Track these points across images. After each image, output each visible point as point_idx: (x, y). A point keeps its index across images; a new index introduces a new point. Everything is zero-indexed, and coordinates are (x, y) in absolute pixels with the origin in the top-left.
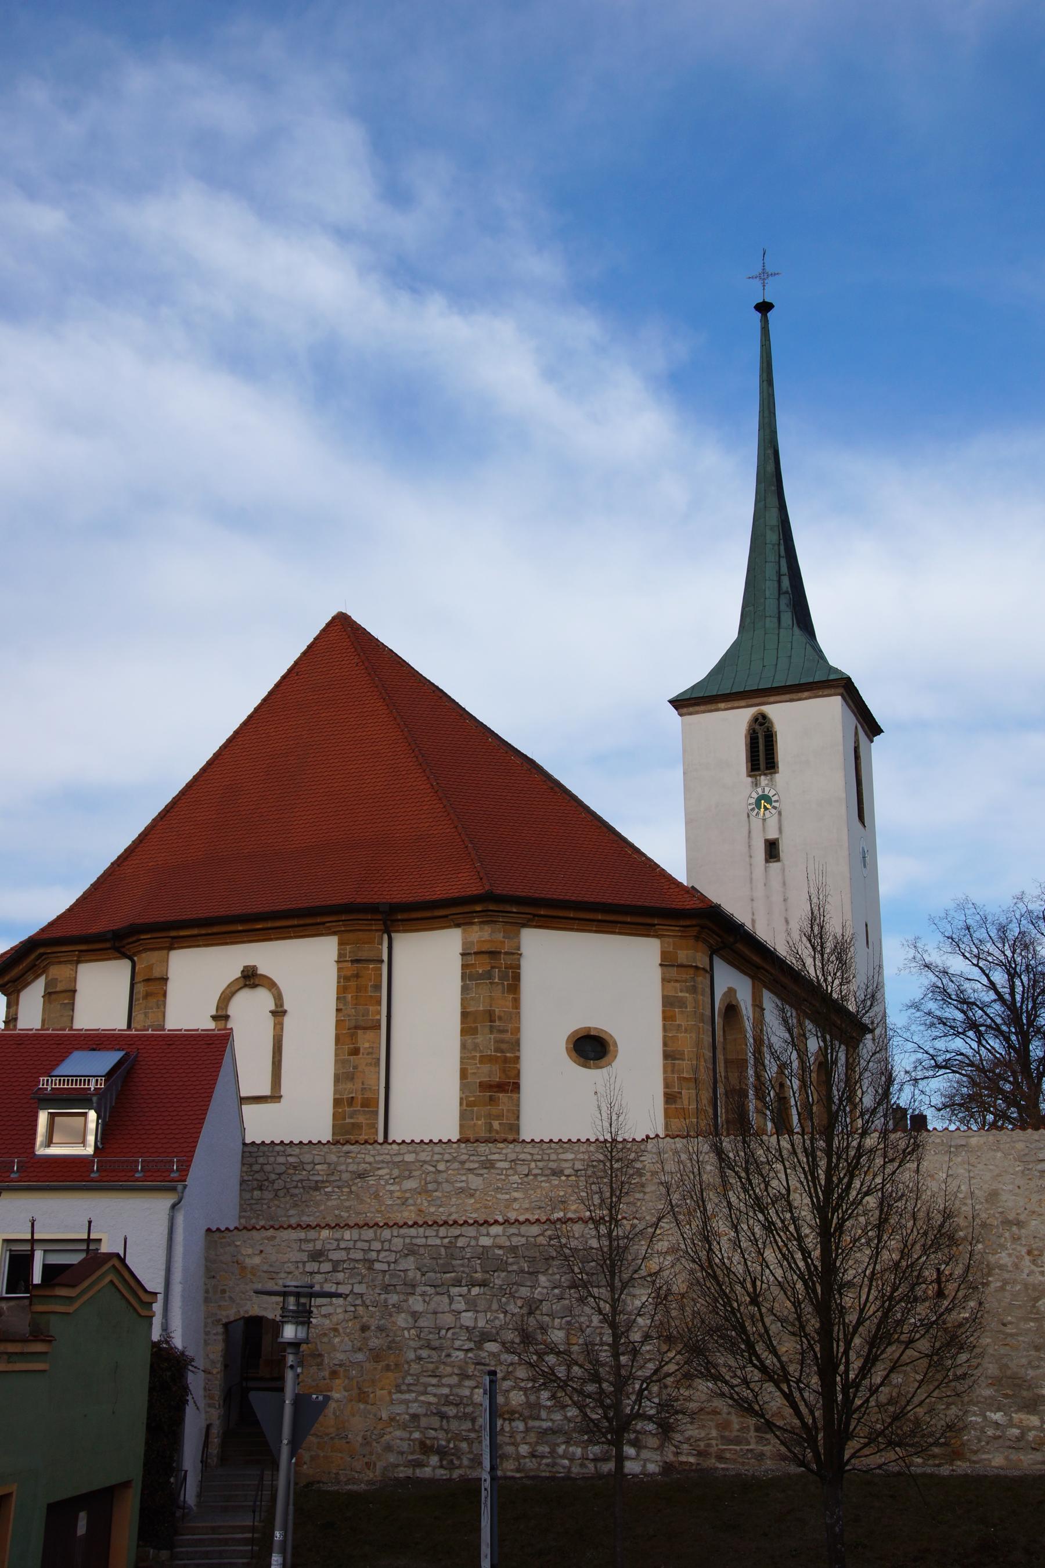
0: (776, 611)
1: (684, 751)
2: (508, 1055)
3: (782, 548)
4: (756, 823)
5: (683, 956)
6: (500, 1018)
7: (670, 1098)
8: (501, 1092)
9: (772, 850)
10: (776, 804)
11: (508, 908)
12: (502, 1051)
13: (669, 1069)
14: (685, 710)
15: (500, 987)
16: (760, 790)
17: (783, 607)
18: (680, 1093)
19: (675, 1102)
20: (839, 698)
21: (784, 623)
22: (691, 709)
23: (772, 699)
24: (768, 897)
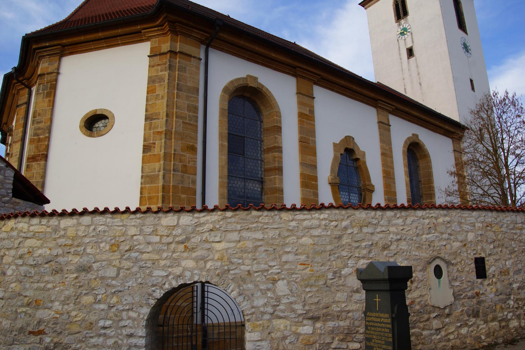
1: (369, 24)
2: (41, 137)
4: (402, 42)
5: (166, 47)
6: (39, 115)
7: (146, 148)
9: (410, 52)
11: (44, 45)
12: (38, 135)
14: (367, 6)
15: (42, 95)
16: (401, 27)
18: (155, 143)
19: (150, 151)
22: (369, 4)
24: (410, 75)
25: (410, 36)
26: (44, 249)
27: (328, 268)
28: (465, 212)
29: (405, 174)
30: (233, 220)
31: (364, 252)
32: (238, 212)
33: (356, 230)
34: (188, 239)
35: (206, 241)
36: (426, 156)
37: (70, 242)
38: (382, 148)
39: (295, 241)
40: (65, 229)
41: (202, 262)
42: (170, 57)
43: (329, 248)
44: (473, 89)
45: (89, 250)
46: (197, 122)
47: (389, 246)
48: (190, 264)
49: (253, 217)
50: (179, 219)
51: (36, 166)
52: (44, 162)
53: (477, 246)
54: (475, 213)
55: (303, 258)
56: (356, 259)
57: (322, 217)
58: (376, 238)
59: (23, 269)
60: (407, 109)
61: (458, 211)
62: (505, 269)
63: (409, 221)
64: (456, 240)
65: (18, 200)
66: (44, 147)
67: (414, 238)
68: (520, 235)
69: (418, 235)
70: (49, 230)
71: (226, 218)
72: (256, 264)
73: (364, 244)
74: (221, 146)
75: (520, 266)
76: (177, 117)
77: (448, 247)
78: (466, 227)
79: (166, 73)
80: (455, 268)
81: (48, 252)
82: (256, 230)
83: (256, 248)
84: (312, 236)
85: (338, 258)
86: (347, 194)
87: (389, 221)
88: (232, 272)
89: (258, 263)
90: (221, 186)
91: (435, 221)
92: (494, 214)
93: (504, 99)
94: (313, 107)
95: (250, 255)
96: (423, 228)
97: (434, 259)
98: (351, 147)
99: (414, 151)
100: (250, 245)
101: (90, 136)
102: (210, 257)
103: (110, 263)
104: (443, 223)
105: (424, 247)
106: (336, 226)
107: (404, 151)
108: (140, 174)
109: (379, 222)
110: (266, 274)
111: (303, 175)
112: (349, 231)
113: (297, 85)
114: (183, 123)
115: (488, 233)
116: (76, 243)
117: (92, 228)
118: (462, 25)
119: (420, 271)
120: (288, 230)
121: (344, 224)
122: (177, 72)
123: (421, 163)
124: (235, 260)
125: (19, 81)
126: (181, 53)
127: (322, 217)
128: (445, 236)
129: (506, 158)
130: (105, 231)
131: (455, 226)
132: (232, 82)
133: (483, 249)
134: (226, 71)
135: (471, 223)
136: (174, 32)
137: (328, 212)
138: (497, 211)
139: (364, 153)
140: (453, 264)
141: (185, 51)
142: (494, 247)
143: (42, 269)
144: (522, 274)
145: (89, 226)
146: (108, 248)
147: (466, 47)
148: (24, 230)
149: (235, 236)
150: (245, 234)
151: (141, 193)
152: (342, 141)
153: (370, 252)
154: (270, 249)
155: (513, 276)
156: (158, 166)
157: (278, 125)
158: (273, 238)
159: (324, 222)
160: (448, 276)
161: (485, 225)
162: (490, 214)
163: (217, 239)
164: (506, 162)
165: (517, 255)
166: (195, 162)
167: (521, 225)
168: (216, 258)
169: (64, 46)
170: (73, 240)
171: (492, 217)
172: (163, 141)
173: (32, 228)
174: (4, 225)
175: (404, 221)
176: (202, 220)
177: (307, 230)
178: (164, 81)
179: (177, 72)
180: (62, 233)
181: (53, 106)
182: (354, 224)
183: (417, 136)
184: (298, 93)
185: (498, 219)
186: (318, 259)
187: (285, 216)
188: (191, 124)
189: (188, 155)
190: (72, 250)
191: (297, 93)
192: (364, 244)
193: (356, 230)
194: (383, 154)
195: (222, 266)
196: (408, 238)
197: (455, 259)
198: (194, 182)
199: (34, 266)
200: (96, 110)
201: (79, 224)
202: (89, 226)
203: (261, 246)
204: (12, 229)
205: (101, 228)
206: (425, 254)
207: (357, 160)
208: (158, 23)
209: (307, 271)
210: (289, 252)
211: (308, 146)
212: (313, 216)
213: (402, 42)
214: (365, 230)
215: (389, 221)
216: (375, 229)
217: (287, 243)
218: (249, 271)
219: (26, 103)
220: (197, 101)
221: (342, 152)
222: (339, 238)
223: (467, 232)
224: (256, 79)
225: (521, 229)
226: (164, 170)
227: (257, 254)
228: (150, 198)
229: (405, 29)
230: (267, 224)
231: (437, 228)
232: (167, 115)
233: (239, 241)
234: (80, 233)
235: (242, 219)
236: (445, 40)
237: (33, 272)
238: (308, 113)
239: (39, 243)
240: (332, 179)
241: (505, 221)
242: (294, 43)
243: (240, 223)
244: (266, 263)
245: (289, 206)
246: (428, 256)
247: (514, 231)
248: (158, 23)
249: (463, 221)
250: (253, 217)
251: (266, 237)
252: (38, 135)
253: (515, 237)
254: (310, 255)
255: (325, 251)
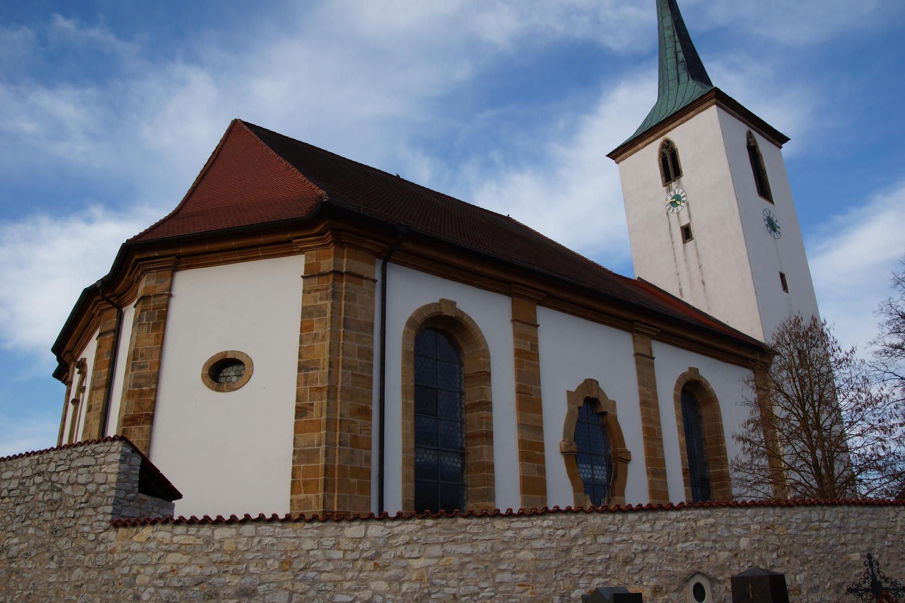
0: (676, 75)
1: (623, 185)
2: (145, 388)
3: (676, 37)
4: (673, 217)
5: (327, 265)
6: (142, 356)
7: (301, 411)
8: (133, 425)
9: (687, 233)
10: (684, 199)
11: (151, 255)
12: (140, 386)
13: (302, 382)
14: (619, 158)
15: (146, 327)
16: (672, 193)
17: (680, 71)
18: (312, 405)
19: (306, 415)
20: (714, 108)
21: (681, 81)
23: (670, 127)
24: (688, 269)
25: (686, 207)
26: (193, 567)
27: (553, 589)
28: (736, 510)
29: (679, 432)
30: (434, 530)
31: (600, 568)
32: (440, 520)
33: (588, 540)
34: (378, 554)
35: (401, 557)
36: (711, 400)
37: (228, 558)
38: (641, 393)
39: (512, 555)
40: (221, 541)
41: (396, 584)
42: (334, 279)
43: (554, 563)
44: (785, 288)
45: (252, 569)
46: (371, 372)
47: (632, 560)
48: (382, 586)
49: (459, 526)
50: (366, 530)
51: (137, 432)
52: (148, 426)
53: (753, 556)
54: (749, 511)
55: (522, 577)
56: (590, 577)
57: (545, 524)
58: (615, 550)
59: (164, 592)
60: (678, 332)
61: (726, 509)
62: (795, 586)
63: (658, 526)
64: (724, 549)
65: (144, 497)
66: (149, 404)
67: (666, 548)
68: (817, 538)
69: (670, 544)
70: (199, 541)
71: (424, 528)
72: (464, 585)
73: (599, 558)
74: (405, 406)
75: (817, 581)
76: (343, 367)
77: (713, 558)
78: (737, 531)
79: (328, 303)
80: (723, 587)
81: (199, 571)
82: (462, 542)
83: (463, 565)
84: (532, 549)
85: (566, 576)
86: (589, 466)
87: (632, 527)
88: (433, 596)
89: (466, 584)
90: (405, 464)
91: (694, 525)
92: (778, 510)
93: (810, 329)
94: (536, 339)
95: (456, 575)
96: (677, 534)
97: (693, 576)
98: (593, 395)
99: (693, 393)
100: (455, 561)
101: (218, 389)
102: (406, 578)
103: (280, 585)
104: (705, 527)
105: (679, 559)
106: (563, 536)
107: (675, 396)
108: (291, 448)
109: (618, 528)
110: (475, 598)
111: (522, 443)
112: (580, 542)
113: (513, 309)
114: (353, 375)
115: (768, 538)
116: (235, 559)
117: (256, 540)
118: (764, 190)
119: (675, 591)
120: (503, 542)
121: (574, 532)
122: (343, 302)
123: (705, 412)
124: (438, 581)
125: (104, 298)
126: (348, 273)
127: (545, 524)
128: (708, 544)
129: (817, 416)
130: (273, 545)
131: (722, 531)
132: (419, 311)
133: (761, 559)
134: (411, 294)
135: (744, 525)
136: (339, 243)
137: (552, 517)
138: (782, 506)
139: (614, 402)
140: (719, 582)
141: (353, 270)
142: (778, 557)
143: (191, 593)
144: (820, 593)
145: (252, 538)
146: (277, 565)
147: (772, 225)
148: (165, 542)
149: (436, 550)
150: (450, 548)
151: (293, 476)
152: (580, 387)
153: (607, 568)
154: (481, 566)
155: (807, 595)
156: (317, 437)
157: (486, 369)
158: (484, 553)
159: (547, 531)
160: (713, 598)
161: (764, 526)
162: (771, 511)
163: (415, 554)
164: (818, 420)
165: (811, 567)
166: (370, 430)
167: (817, 523)
168: (414, 578)
169: (179, 257)
170: (231, 555)
171: (774, 515)
172: (325, 401)
173: (176, 539)
174: (137, 533)
175: (652, 526)
176: (396, 530)
177: (526, 542)
178: (325, 315)
179: (343, 302)
180: (217, 546)
181: (162, 344)
182: (586, 532)
183: (696, 371)
184: (515, 320)
185: (784, 518)
186: (541, 578)
187: (499, 524)
188: (363, 377)
189: (360, 421)
190: (231, 568)
191: (513, 321)
192: (599, 558)
193: (588, 540)
194: (643, 403)
195: (421, 588)
196: (658, 548)
197: (722, 574)
198: (368, 460)
199: (179, 589)
200: (226, 352)
201: (239, 535)
202: (252, 538)
203: (469, 562)
204: (148, 539)
205: (267, 541)
206: (681, 569)
207: (604, 414)
208: (316, 231)
209: (528, 594)
210: (504, 570)
211: (529, 399)
212: (534, 523)
213: (673, 217)
214: (601, 539)
215: (632, 527)
216: (614, 537)
217: (502, 559)
218: (454, 595)
219: (114, 331)
220: (372, 342)
221: (581, 403)
222: (568, 550)
223: (739, 537)
224: (453, 304)
225: (818, 530)
226: (326, 443)
227: (465, 573)
228: (306, 484)
229: (678, 198)
230: (476, 534)
231: (697, 534)
232: (330, 365)
233: (442, 557)
234: (241, 547)
235: (445, 529)
236: (738, 216)
237: (178, 596)
238: (529, 349)
239: (185, 559)
240: (565, 446)
241: (793, 520)
242: (508, 218)
243: (443, 534)
244: (476, 585)
245: (503, 511)
246: (684, 571)
247: (807, 533)
248: (316, 231)
249: (733, 522)
250: (459, 526)
251: (476, 551)
252: (140, 386)
253: (809, 540)
254: (531, 573)
255: (550, 568)
